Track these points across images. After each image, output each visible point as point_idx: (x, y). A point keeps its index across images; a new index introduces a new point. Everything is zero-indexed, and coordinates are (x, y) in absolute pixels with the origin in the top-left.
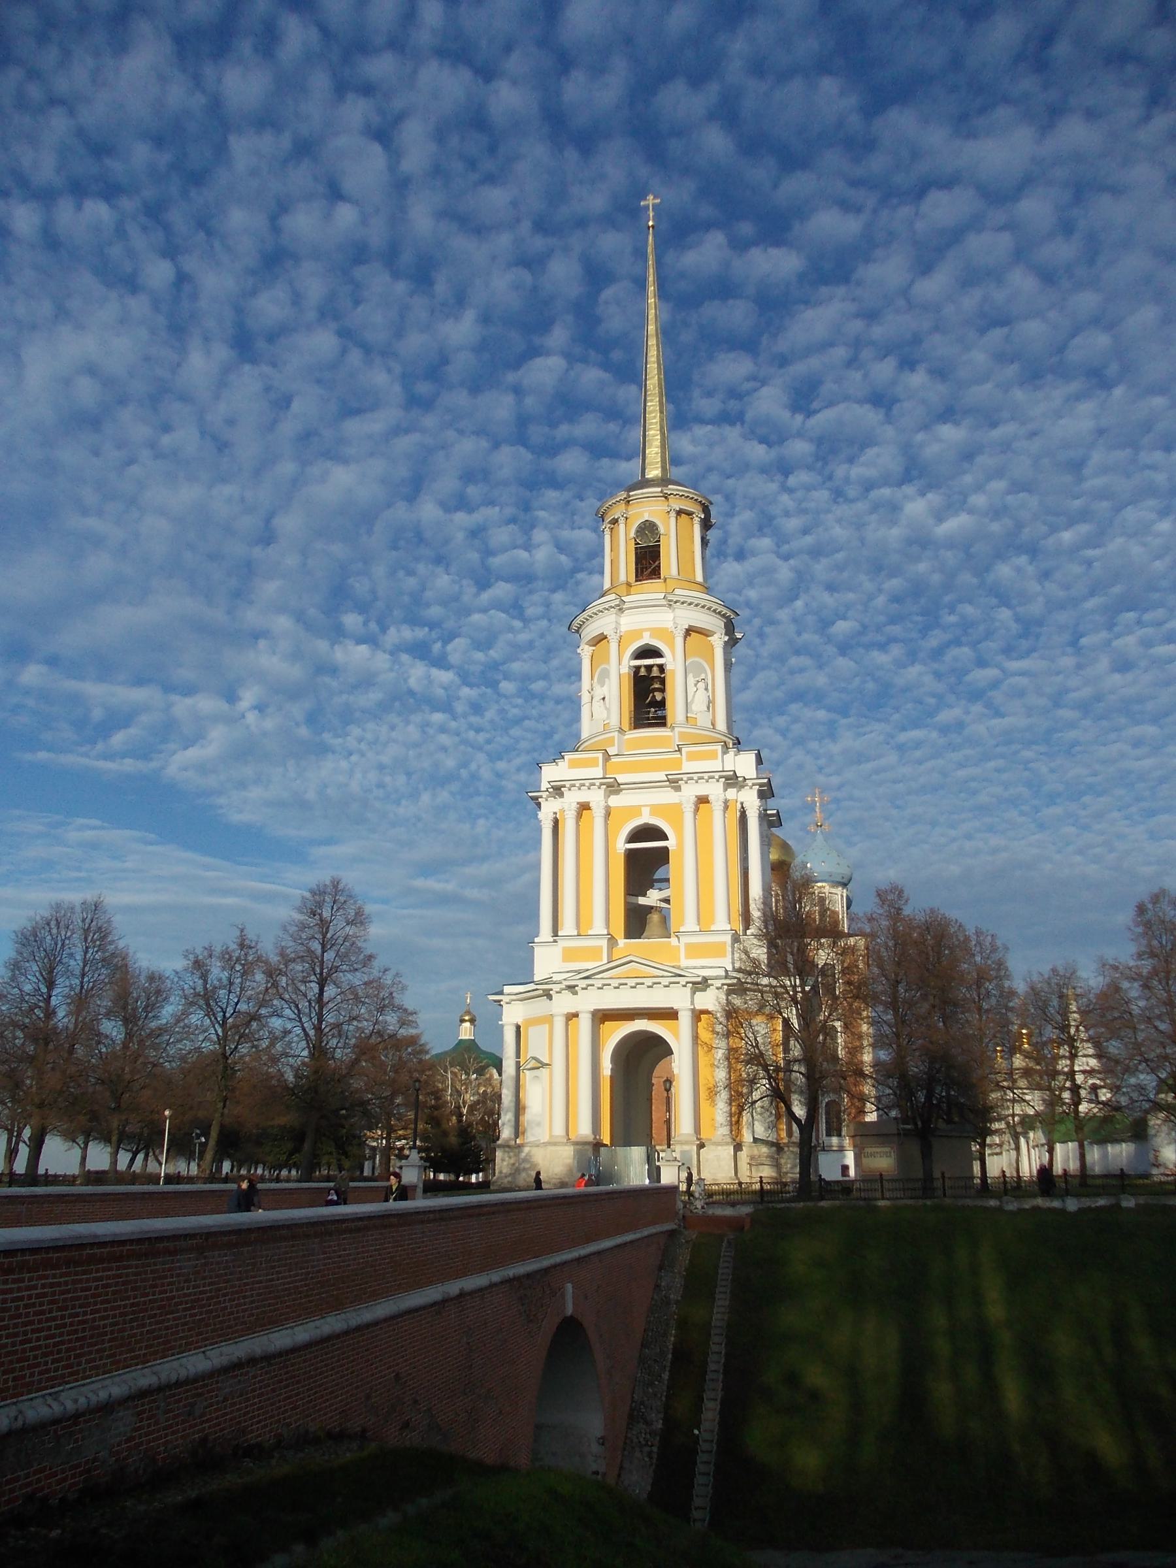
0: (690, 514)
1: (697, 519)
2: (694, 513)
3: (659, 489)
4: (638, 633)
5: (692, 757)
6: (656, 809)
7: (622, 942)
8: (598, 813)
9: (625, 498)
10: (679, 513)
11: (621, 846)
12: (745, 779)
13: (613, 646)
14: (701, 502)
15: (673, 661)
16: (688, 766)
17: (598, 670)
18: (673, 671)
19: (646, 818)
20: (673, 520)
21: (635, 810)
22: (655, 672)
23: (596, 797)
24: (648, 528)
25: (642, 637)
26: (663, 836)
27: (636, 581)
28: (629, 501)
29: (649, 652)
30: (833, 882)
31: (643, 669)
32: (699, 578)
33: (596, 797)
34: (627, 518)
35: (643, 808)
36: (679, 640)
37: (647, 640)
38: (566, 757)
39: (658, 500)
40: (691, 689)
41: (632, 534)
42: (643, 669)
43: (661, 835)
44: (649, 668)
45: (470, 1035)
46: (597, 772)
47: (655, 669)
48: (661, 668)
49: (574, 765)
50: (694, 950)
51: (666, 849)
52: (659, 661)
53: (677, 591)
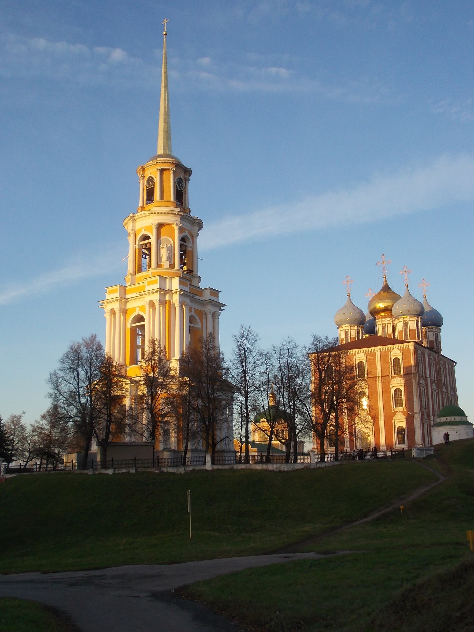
0: (169, 169)
1: (171, 171)
2: (170, 169)
3: (151, 162)
4: (140, 230)
5: (149, 284)
9: (141, 168)
10: (162, 171)
12: (172, 291)
14: (175, 163)
15: (153, 240)
16: (148, 288)
20: (158, 175)
21: (134, 309)
24: (151, 180)
27: (147, 204)
28: (144, 169)
30: (410, 314)
32: (172, 198)
34: (144, 177)
35: (136, 308)
37: (143, 232)
38: (107, 290)
39: (154, 166)
44: (146, 244)
48: (150, 243)
52: (149, 241)
53: (154, 208)
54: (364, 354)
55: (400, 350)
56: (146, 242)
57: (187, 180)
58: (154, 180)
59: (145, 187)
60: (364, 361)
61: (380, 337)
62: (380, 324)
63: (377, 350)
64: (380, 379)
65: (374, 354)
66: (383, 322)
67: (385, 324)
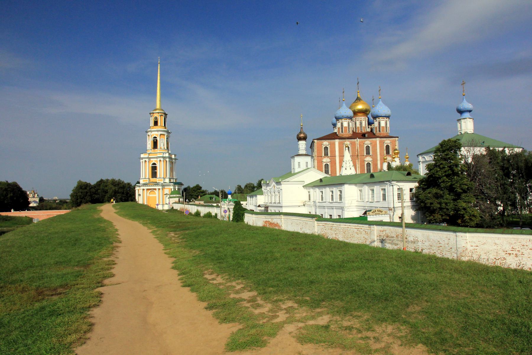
4: (153, 135)
6: (155, 161)
7: (151, 179)
8: (147, 162)
11: (151, 165)
15: (158, 139)
19: (154, 162)
23: (147, 160)
24: (156, 118)
26: (156, 165)
29: (155, 137)
32: (163, 125)
33: (147, 160)
36: (159, 136)
40: (161, 143)
43: (155, 164)
46: (147, 156)
49: (144, 155)
50: (159, 180)
57: (166, 117)
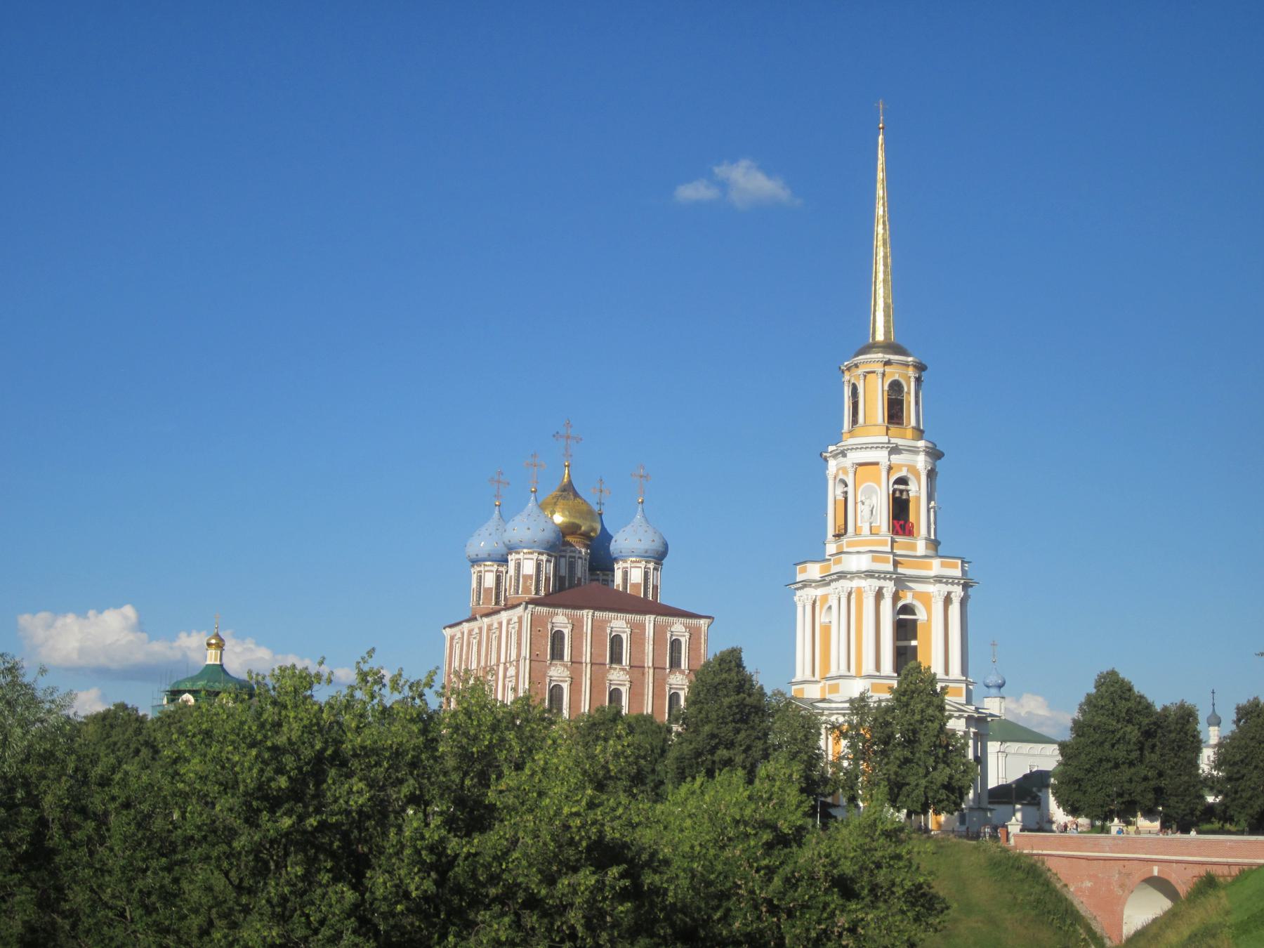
4: (900, 467)
6: (917, 595)
13: (884, 474)
15: (917, 490)
17: (862, 487)
18: (918, 498)
22: (904, 497)
25: (901, 470)
29: (902, 481)
31: (897, 492)
37: (903, 473)
41: (886, 388)
42: (897, 492)
44: (901, 491)
45: (216, 660)
47: (905, 493)
48: (908, 491)
51: (915, 621)
54: (627, 623)
55: (686, 628)
56: (902, 487)
58: (903, 387)
59: (886, 393)
60: (624, 636)
61: (617, 591)
62: (565, 557)
63: (649, 621)
64: (651, 671)
65: (642, 627)
66: (573, 554)
67: (574, 557)
